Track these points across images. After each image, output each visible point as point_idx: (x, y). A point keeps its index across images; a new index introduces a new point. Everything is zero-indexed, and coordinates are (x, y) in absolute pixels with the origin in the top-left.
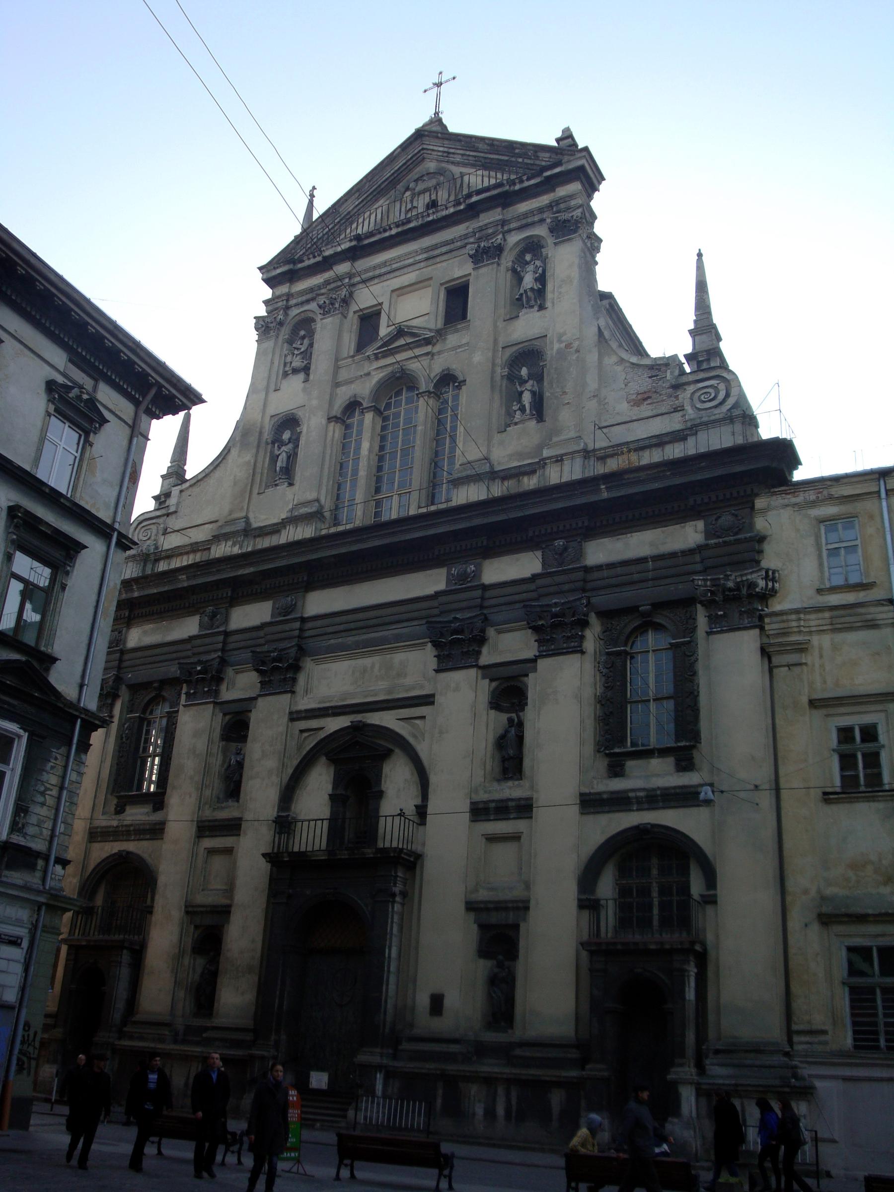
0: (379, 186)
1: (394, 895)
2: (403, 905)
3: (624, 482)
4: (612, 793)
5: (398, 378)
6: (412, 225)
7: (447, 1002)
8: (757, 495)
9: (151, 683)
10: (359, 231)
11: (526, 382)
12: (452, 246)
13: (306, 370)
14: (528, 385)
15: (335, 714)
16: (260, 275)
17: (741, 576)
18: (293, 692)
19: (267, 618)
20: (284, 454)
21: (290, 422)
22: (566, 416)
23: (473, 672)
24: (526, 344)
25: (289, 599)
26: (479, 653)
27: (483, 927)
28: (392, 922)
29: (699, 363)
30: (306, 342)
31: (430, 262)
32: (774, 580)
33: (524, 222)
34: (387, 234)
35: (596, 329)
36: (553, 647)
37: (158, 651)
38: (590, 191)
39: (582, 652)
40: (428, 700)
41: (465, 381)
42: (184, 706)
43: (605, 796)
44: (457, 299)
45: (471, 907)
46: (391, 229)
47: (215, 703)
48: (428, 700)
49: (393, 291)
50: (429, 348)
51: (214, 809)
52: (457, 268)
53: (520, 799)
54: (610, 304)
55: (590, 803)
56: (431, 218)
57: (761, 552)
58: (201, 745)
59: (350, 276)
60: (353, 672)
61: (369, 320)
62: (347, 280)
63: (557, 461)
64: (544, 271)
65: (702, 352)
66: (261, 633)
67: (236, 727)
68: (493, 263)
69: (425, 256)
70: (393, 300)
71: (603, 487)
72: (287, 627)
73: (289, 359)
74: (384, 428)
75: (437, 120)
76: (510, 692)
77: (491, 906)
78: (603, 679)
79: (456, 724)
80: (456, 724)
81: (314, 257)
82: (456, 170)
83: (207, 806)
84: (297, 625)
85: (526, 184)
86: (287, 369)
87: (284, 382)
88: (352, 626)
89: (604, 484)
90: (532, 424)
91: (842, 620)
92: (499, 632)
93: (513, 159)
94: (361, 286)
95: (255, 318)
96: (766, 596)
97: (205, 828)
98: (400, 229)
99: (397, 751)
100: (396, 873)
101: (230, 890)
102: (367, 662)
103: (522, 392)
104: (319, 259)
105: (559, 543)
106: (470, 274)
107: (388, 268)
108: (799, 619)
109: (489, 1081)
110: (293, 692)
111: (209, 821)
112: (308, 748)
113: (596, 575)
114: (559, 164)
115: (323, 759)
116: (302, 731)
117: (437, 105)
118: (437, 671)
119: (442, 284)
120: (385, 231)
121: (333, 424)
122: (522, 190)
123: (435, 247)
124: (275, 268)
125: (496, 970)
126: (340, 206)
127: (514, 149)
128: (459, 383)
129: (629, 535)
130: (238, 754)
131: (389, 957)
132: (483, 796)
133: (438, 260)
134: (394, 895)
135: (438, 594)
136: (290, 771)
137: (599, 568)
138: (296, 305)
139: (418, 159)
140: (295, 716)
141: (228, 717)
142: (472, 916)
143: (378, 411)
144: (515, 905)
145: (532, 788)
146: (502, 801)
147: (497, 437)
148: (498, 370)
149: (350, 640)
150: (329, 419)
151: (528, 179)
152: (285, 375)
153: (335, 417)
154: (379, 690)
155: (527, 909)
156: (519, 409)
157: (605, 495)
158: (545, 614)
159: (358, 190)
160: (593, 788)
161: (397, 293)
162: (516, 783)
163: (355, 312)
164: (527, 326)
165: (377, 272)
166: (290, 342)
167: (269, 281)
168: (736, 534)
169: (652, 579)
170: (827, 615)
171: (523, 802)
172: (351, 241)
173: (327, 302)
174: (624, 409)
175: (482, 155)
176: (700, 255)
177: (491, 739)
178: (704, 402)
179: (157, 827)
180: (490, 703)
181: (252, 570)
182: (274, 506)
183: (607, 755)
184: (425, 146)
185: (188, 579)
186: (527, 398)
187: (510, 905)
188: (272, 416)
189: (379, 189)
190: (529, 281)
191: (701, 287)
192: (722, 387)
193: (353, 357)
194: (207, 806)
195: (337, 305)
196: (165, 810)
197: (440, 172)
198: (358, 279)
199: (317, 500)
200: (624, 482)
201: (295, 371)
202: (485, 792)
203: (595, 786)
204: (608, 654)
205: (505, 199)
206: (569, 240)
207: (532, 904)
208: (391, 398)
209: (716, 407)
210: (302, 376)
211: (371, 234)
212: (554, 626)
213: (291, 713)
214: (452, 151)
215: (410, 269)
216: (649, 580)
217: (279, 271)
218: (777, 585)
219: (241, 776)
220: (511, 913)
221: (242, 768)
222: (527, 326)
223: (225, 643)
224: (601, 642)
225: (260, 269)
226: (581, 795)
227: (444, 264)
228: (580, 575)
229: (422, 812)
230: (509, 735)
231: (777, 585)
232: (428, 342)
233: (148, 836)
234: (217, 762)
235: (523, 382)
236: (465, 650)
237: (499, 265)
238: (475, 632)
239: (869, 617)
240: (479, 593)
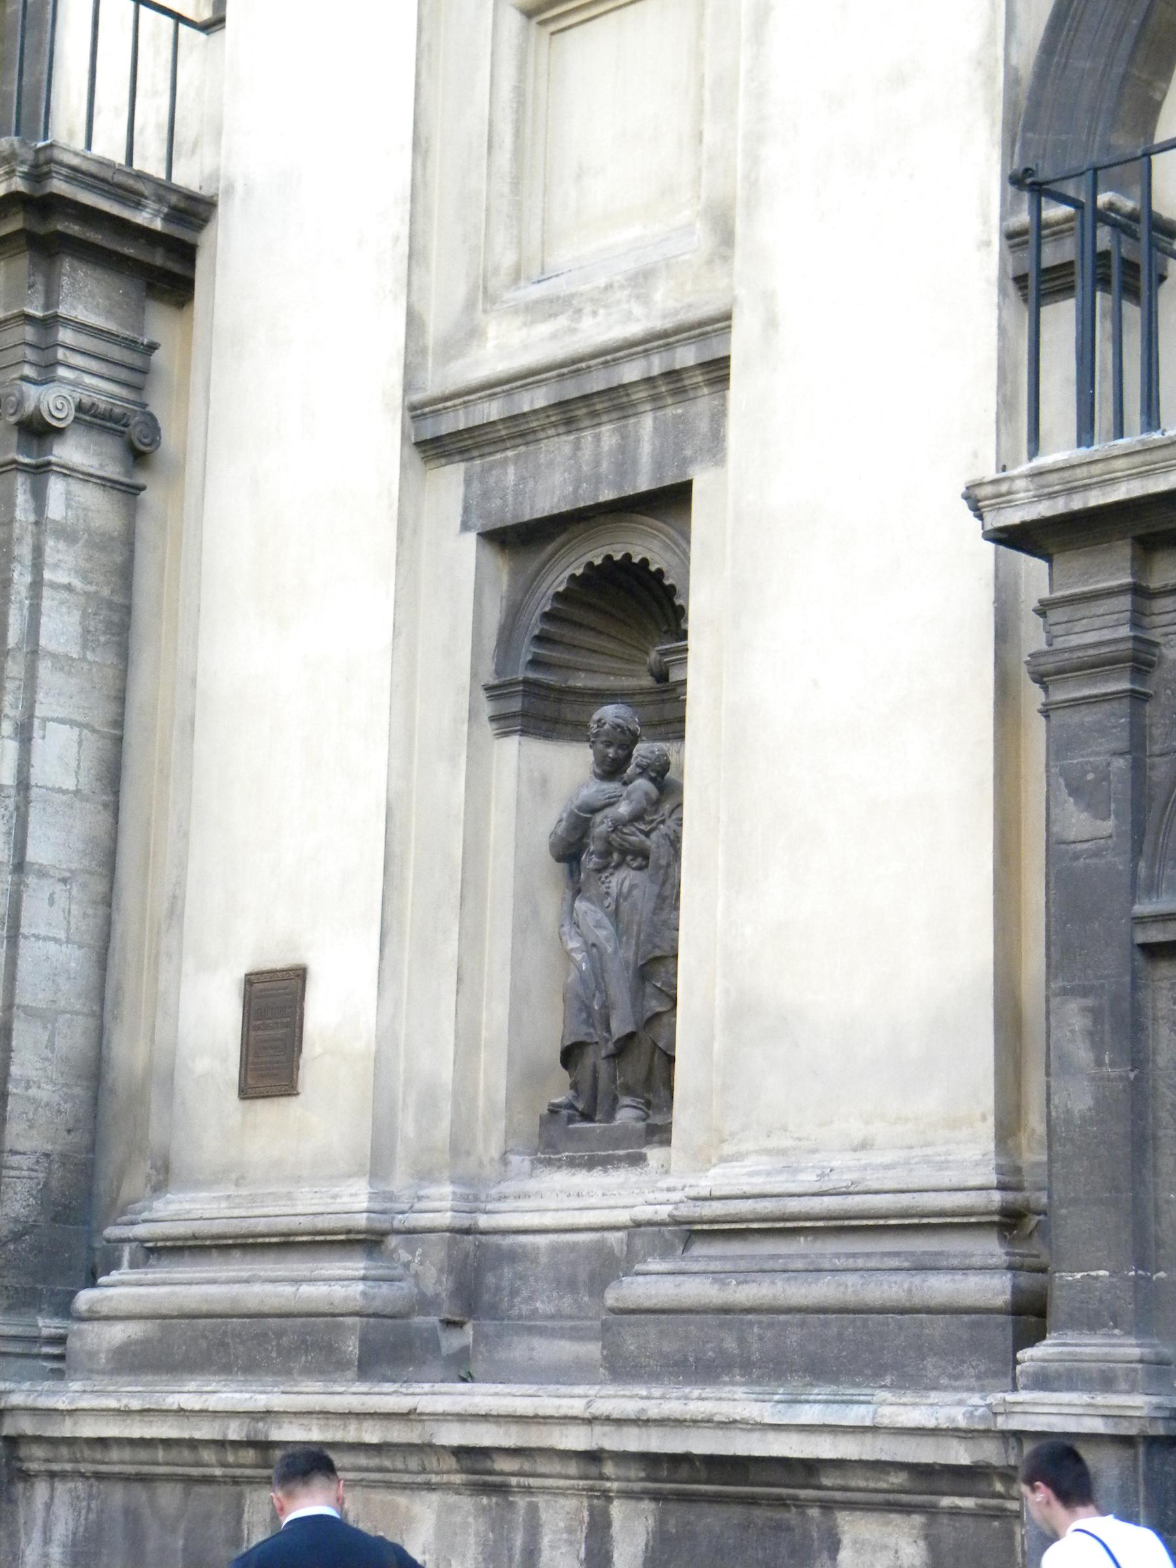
1: (38, 431)
7: (321, 1014)
77: (537, 399)
100: (50, 300)
109: (480, 1471)
125: (595, 790)
142: (450, 482)
144: (657, 365)
155: (717, 371)
187: (631, 372)
207: (741, 346)
220: (646, 424)
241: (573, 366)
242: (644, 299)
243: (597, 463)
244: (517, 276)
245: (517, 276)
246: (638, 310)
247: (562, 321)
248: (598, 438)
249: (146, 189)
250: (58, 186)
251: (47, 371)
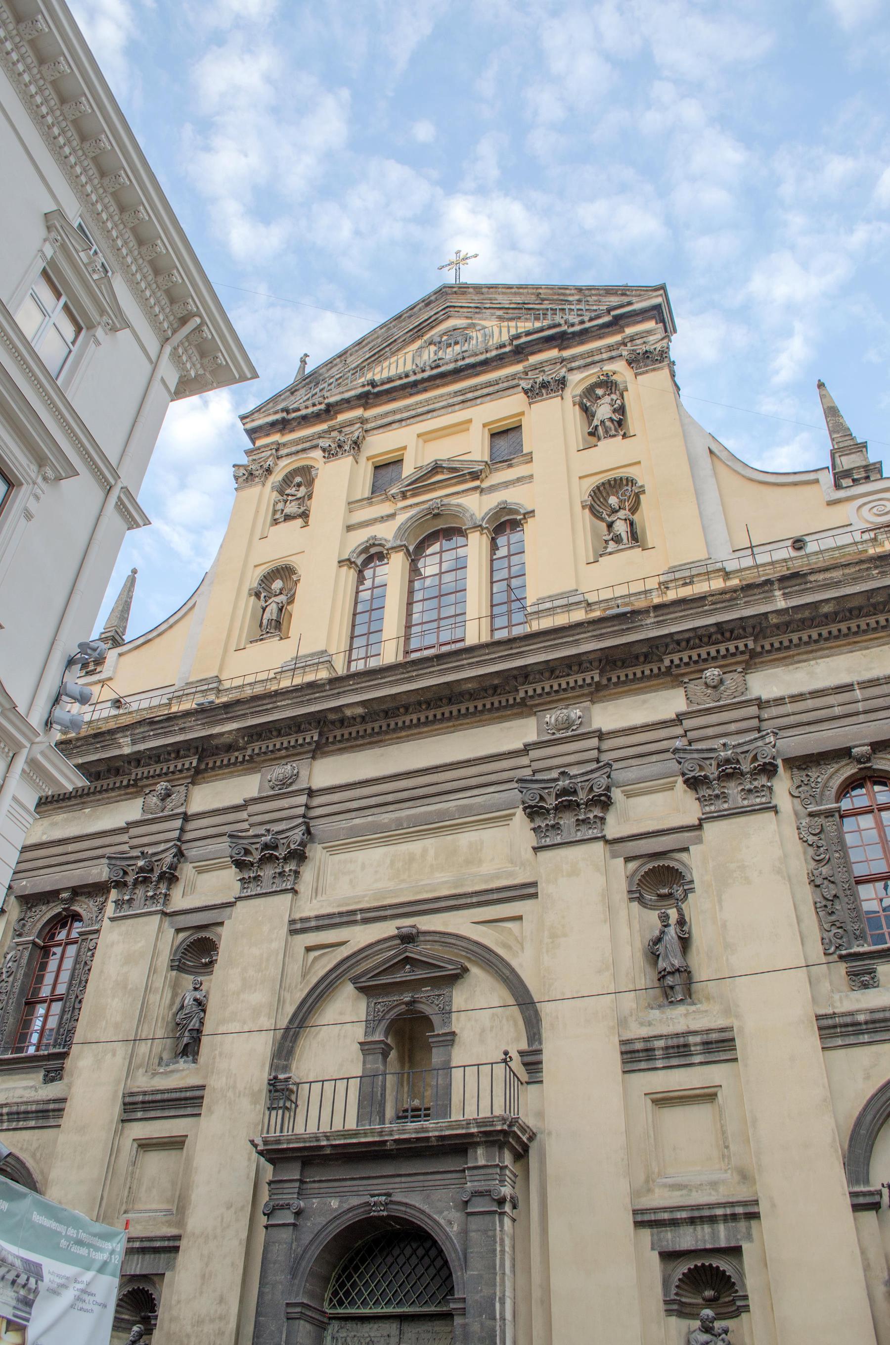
2: (514, 1220)
3: (809, 585)
4: (872, 1011)
9: (57, 892)
10: (377, 378)
11: (617, 511)
12: (496, 387)
13: (305, 515)
14: (622, 514)
15: (366, 921)
18: (295, 892)
19: (255, 794)
20: (274, 606)
21: (284, 572)
23: (599, 846)
25: (289, 767)
26: (603, 820)
27: (669, 1256)
28: (503, 1251)
30: (303, 491)
31: (469, 404)
33: (589, 360)
36: (726, 806)
37: (71, 848)
39: (775, 809)
40: (526, 891)
41: (533, 511)
42: (112, 919)
43: (861, 1018)
44: (505, 435)
45: (646, 1221)
47: (165, 914)
48: (526, 891)
49: (419, 436)
50: (477, 483)
51: (154, 1075)
52: (507, 406)
53: (709, 1031)
55: (836, 1030)
56: (467, 361)
58: (137, 975)
59: (363, 421)
60: (392, 862)
61: (387, 467)
62: (358, 425)
65: (858, 468)
66: (244, 815)
67: (198, 950)
71: (778, 593)
72: (285, 803)
73: (280, 506)
76: (660, 878)
77: (684, 1215)
78: (811, 851)
79: (577, 925)
80: (577, 925)
81: (314, 405)
83: (141, 1071)
84: (303, 799)
85: (587, 325)
86: (277, 516)
87: (273, 528)
88: (390, 798)
89: (780, 589)
92: (628, 796)
94: (375, 432)
95: (234, 466)
97: (136, 1107)
99: (475, 970)
100: (501, 1159)
101: (179, 1208)
102: (415, 847)
103: (613, 522)
105: (712, 673)
106: (523, 413)
107: (413, 413)
110: (295, 892)
111: (145, 1093)
112: (322, 973)
113: (774, 711)
115: (349, 989)
116: (309, 949)
118: (536, 849)
119: (484, 426)
120: (407, 376)
121: (345, 568)
123: (474, 389)
128: (524, 514)
129: (812, 663)
130: (196, 989)
131: (503, 1319)
132: (636, 1031)
134: (501, 1202)
135: (527, 749)
136: (290, 1009)
137: (779, 701)
138: (287, 455)
140: (298, 927)
141: (182, 936)
142: (646, 1234)
144: (729, 1211)
145: (727, 1011)
146: (677, 1035)
149: (385, 817)
151: (591, 320)
152: (275, 522)
153: (349, 560)
154: (441, 882)
155: (755, 1216)
156: (612, 539)
157: (781, 604)
158: (708, 762)
160: (834, 1007)
162: (693, 1008)
163: (368, 459)
164: (610, 455)
165: (398, 417)
166: (281, 492)
167: (252, 433)
169: (865, 712)
171: (714, 1036)
172: (364, 386)
173: (333, 446)
177: (638, 945)
179: (52, 1106)
180: (630, 892)
181: (234, 726)
182: (258, 665)
183: (841, 957)
185: (134, 742)
186: (621, 528)
187: (719, 1212)
188: (255, 566)
190: (603, 411)
191: (832, 412)
193: (368, 499)
194: (141, 1071)
195: (347, 448)
196: (66, 1080)
198: (373, 425)
200: (809, 585)
201: (288, 518)
202: (642, 1024)
203: (838, 1004)
204: (811, 815)
205: (561, 340)
206: (654, 370)
207: (763, 1208)
210: (299, 522)
211: (390, 380)
212: (725, 777)
213: (292, 922)
216: (857, 714)
219: (202, 1023)
221: (204, 1011)
222: (610, 455)
223: (182, 830)
224: (797, 801)
226: (818, 1017)
228: (753, 710)
229: (533, 1064)
230: (666, 938)
232: (475, 476)
233: (32, 1123)
234: (161, 1005)
235: (615, 511)
236: (581, 817)
238: (600, 791)
240: (594, 742)
241: (698, 1207)
242: (717, 1191)
243: (704, 1236)
244: (659, 1175)
245: (659, 1175)
246: (713, 1193)
247: (684, 1192)
248: (703, 1229)
249: (528, 1131)
250: (515, 1129)
251: (502, 1181)
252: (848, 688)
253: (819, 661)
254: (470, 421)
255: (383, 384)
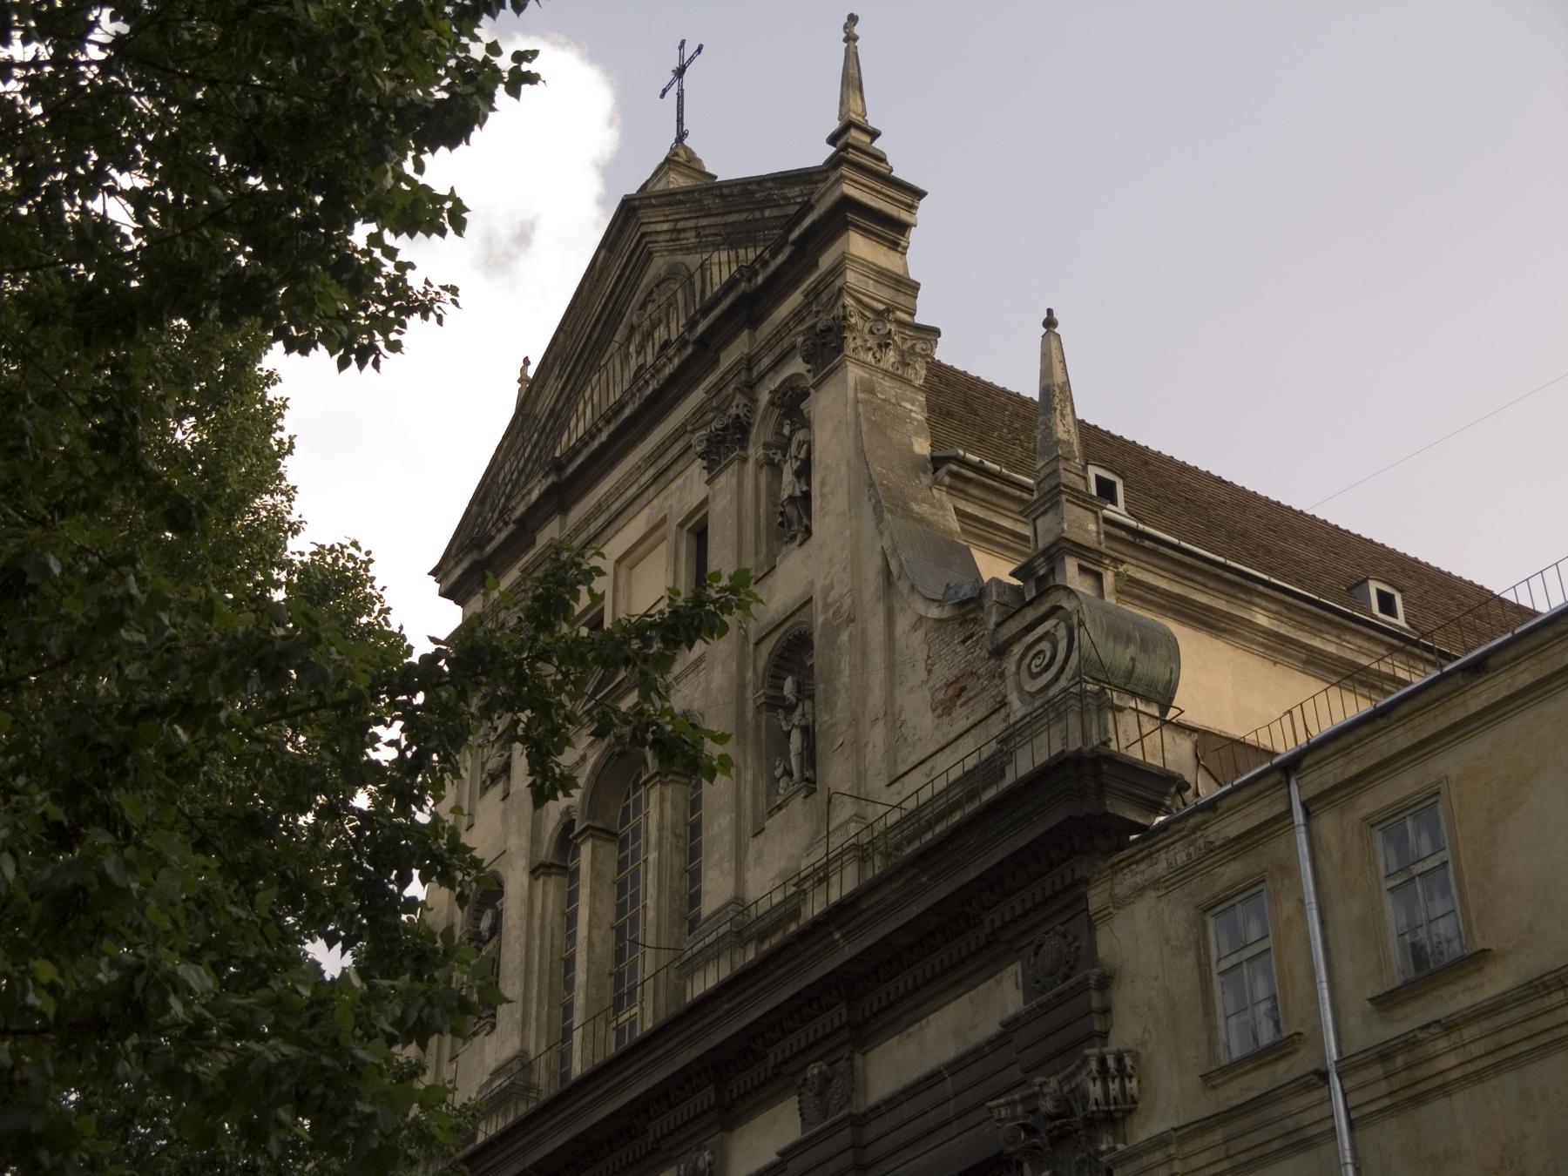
0: (589, 337)
3: (865, 916)
5: (622, 754)
6: (627, 412)
8: (1087, 882)
11: (795, 707)
16: (434, 586)
17: (1068, 1078)
22: (836, 773)
24: (788, 625)
29: (1041, 580)
31: (662, 481)
32: (1122, 1073)
33: (778, 351)
34: (596, 444)
35: (878, 560)
38: (891, 235)
46: (600, 431)
54: (953, 475)
57: (1106, 1011)
63: (820, 881)
64: (809, 452)
68: (731, 462)
69: (651, 472)
70: (622, 581)
74: (622, 865)
75: (680, 159)
82: (694, 260)
85: (773, 265)
90: (798, 803)
91: (1244, 1143)
93: (758, 215)
96: (1115, 1117)
98: (612, 428)
103: (788, 735)
104: (512, 527)
108: (1170, 1160)
114: (807, 207)
117: (680, 121)
119: (681, 526)
120: (593, 437)
122: (767, 281)
124: (457, 564)
126: (535, 403)
127: (753, 193)
133: (671, 474)
137: (877, 1111)
139: (642, 257)
143: (606, 834)
147: (753, 846)
148: (749, 693)
150: (538, 870)
151: (774, 255)
152: (485, 789)
153: (542, 865)
157: (849, 951)
159: (555, 360)
161: (626, 562)
165: (593, 528)
168: (1067, 977)
169: (958, 1117)
170: (1218, 1136)
174: (923, 724)
175: (718, 220)
176: (1050, 323)
178: (1040, 674)
184: (644, 229)
189: (591, 344)
192: (1062, 633)
197: (673, 273)
199: (521, 1055)
200: (865, 916)
201: (494, 778)
205: (748, 306)
206: (833, 371)
208: (628, 797)
209: (1056, 678)
214: (680, 225)
215: (636, 506)
217: (459, 571)
218: (1132, 1086)
225: (433, 573)
227: (679, 482)
228: (846, 1135)
231: (1132, 1086)
237: (745, 460)
239: (1290, 1124)
252: (932, 1080)
253: (931, 1018)
254: (663, 520)
255: (570, 460)
